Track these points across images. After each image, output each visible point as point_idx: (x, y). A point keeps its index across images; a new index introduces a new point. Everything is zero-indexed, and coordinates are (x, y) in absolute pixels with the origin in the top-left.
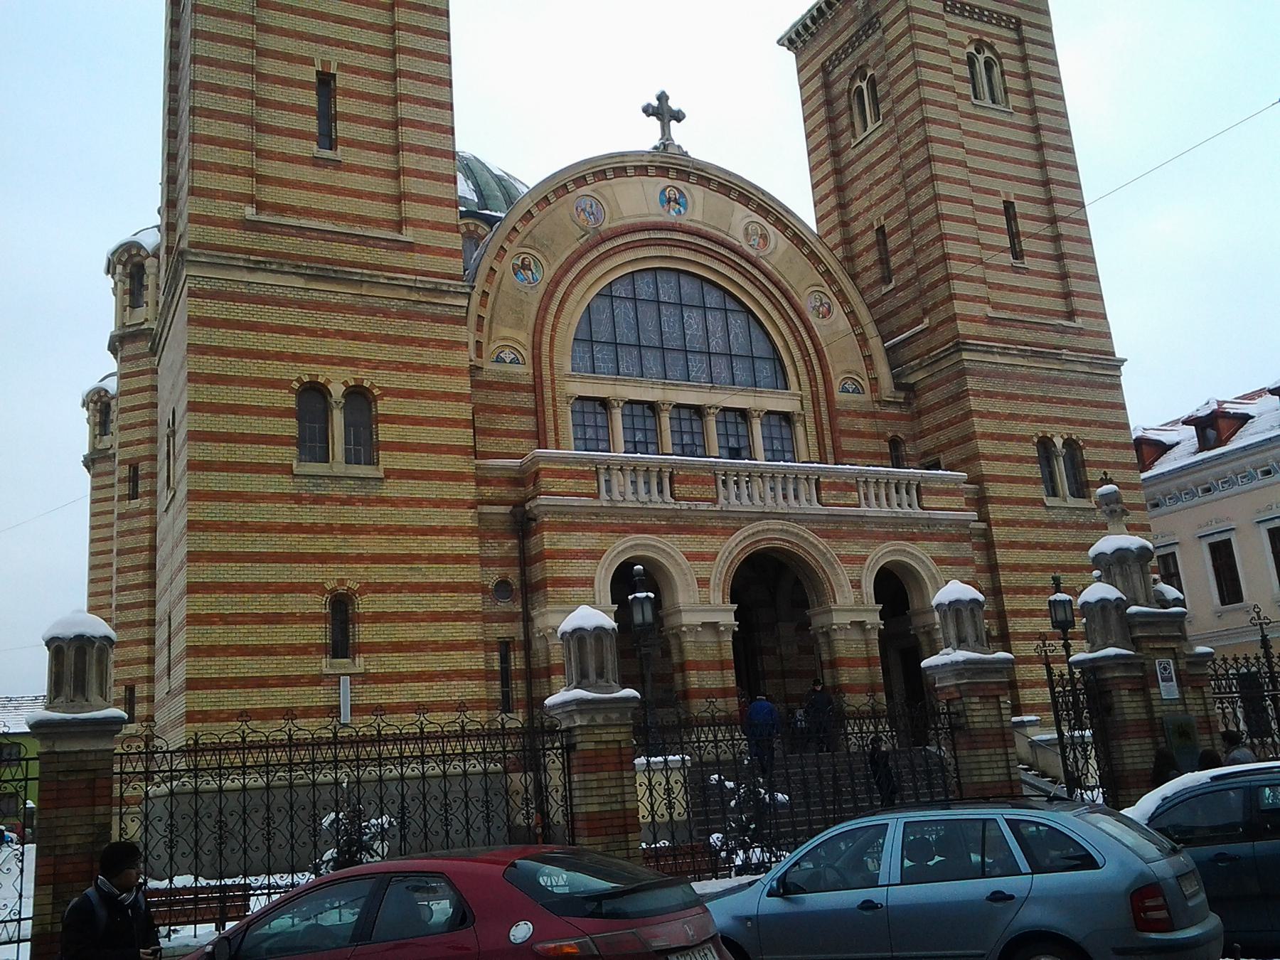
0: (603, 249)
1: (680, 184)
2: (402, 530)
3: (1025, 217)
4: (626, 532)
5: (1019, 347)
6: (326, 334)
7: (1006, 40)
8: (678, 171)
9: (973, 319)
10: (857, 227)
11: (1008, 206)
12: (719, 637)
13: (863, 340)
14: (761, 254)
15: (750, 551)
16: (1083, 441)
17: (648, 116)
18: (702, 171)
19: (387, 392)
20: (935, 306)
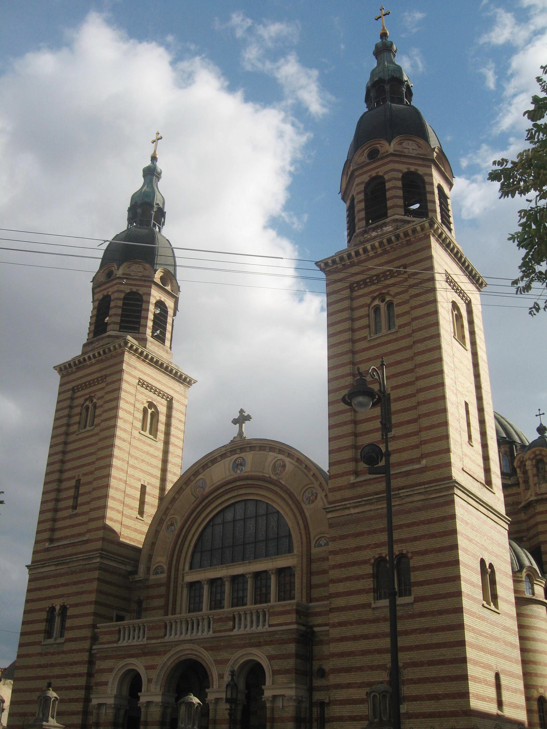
2: (66, 664)
4: (124, 658)
5: (364, 499)
15: (177, 662)
16: (412, 553)
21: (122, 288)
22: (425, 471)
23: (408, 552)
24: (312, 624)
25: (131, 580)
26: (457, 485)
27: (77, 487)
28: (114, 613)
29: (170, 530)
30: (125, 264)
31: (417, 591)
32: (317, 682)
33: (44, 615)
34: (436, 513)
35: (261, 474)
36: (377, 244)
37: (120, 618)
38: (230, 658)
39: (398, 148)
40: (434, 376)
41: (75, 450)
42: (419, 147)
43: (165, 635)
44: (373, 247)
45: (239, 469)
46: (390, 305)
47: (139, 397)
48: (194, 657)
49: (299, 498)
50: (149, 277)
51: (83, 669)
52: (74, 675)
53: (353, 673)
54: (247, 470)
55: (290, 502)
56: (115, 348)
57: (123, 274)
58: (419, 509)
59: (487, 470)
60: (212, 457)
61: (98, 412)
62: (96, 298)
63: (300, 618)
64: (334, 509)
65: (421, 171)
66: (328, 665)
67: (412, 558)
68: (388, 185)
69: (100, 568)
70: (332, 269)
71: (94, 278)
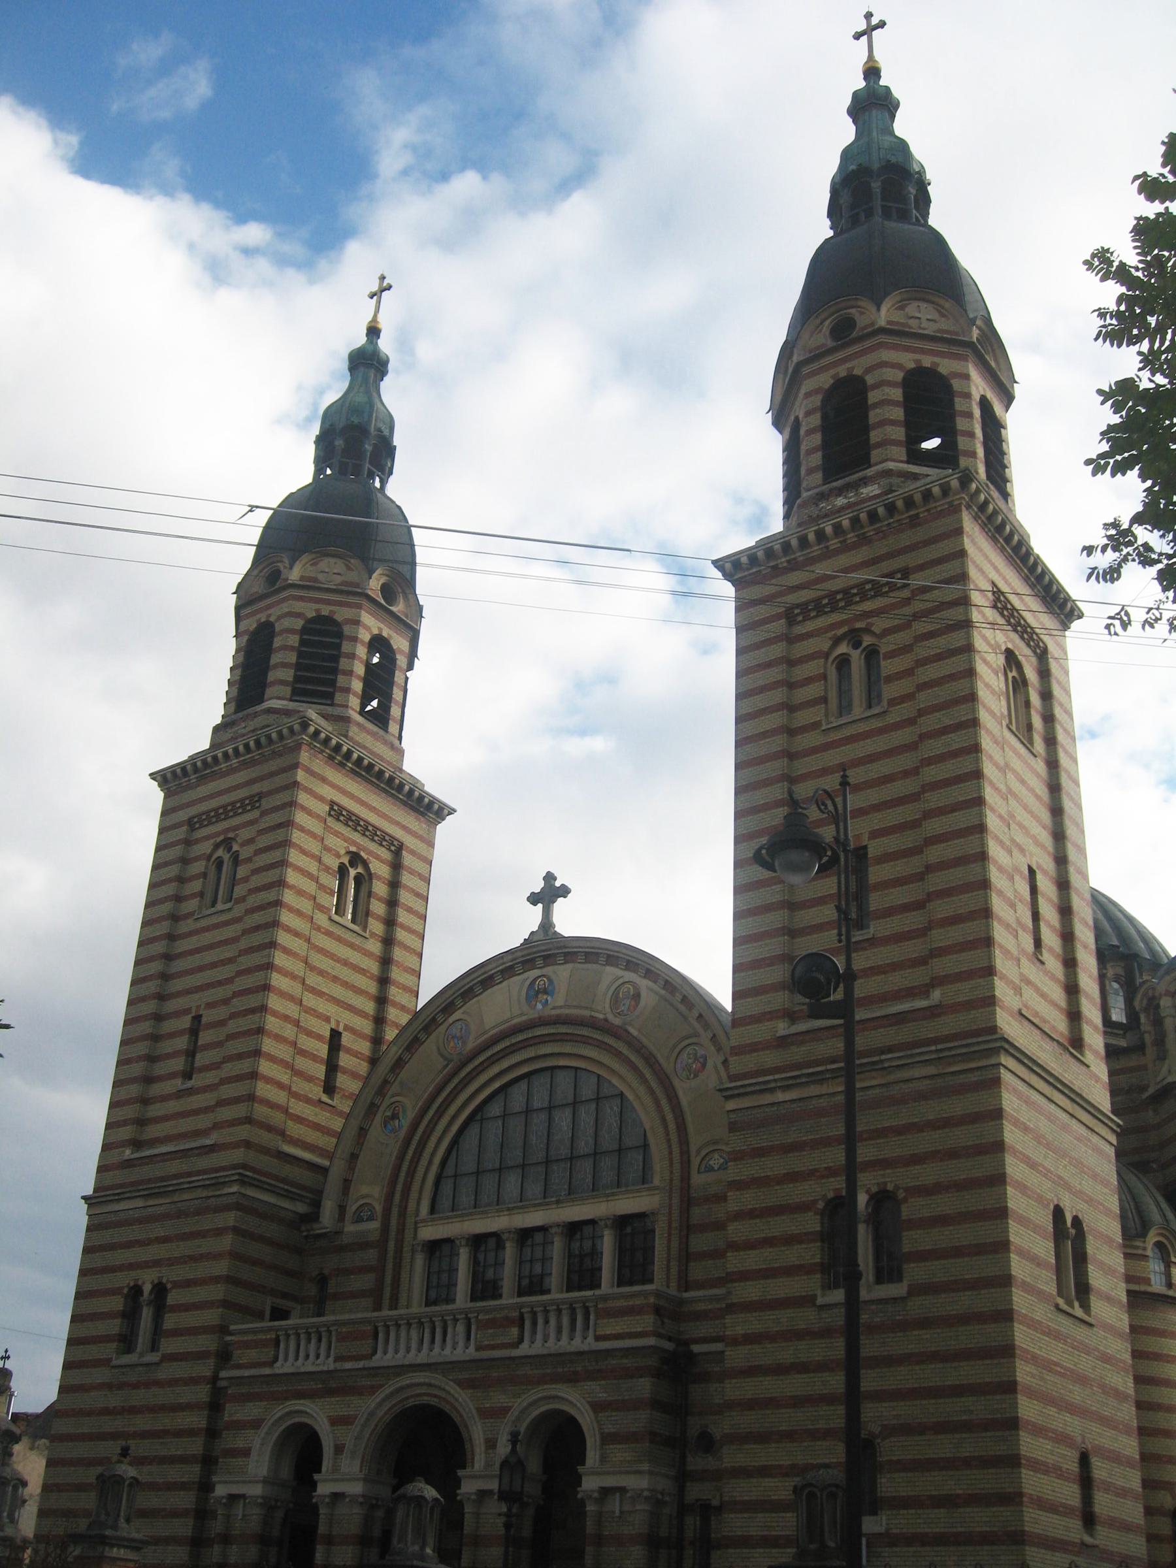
4: (286, 1399)
6: (149, 1242)
16: (907, 1190)
19: (177, 1285)
21: (299, 606)
22: (939, 1015)
23: (897, 1188)
24: (688, 1336)
25: (305, 1234)
26: (1007, 1046)
27: (194, 1032)
28: (268, 1303)
29: (389, 1127)
30: (305, 558)
31: (915, 1272)
32: (696, 1462)
33: (117, 1303)
34: (957, 1106)
35: (587, 1013)
36: (846, 523)
37: (279, 1314)
38: (510, 1404)
39: (898, 317)
40: (962, 809)
41: (191, 952)
42: (943, 315)
43: (375, 1352)
44: (838, 529)
45: (541, 1002)
46: (872, 654)
47: (332, 841)
48: (434, 1401)
49: (668, 1066)
50: (357, 585)
51: (198, 1420)
52: (179, 1433)
53: (773, 1445)
54: (557, 1002)
55: (648, 1074)
56: (281, 737)
57: (302, 578)
58: (922, 1096)
59: (1074, 1016)
60: (483, 974)
61: (242, 872)
62: (242, 628)
63: (663, 1323)
64: (742, 1090)
65: (946, 366)
66: (721, 1427)
67: (905, 1200)
68: (873, 397)
69: (238, 1207)
70: (750, 575)
71: (240, 585)
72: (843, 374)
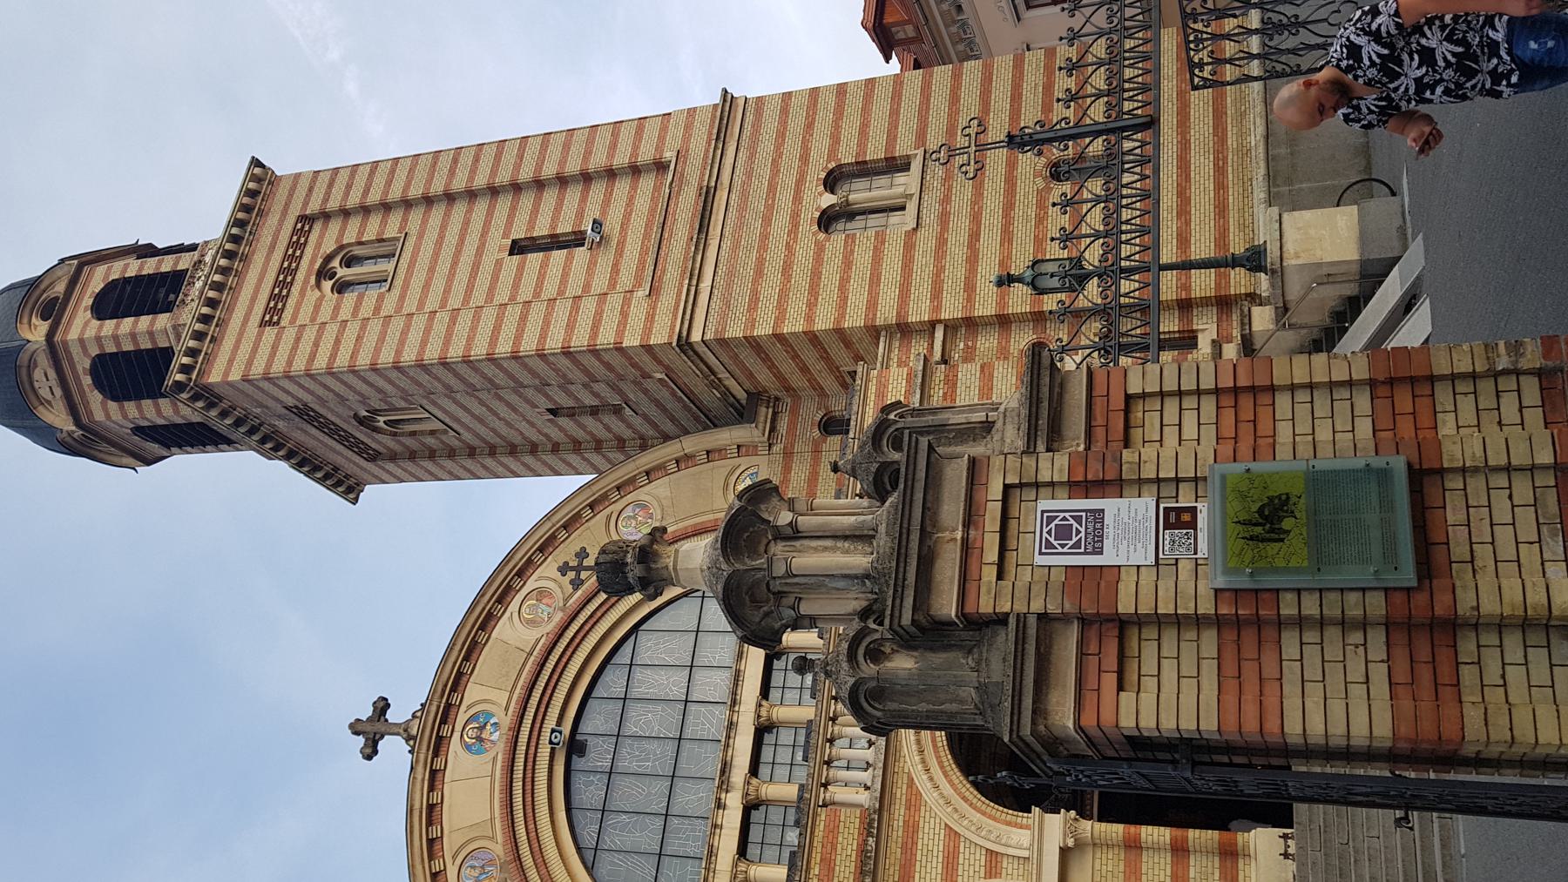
0: (528, 861)
1: (462, 718)
3: (532, 224)
7: (321, 236)
8: (444, 721)
9: (650, 318)
10: (555, 434)
11: (518, 248)
12: (1086, 844)
13: (683, 461)
14: (561, 604)
16: (829, 161)
17: (375, 752)
18: (446, 686)
20: (635, 365)
22: (687, 151)
72: (91, 301)
